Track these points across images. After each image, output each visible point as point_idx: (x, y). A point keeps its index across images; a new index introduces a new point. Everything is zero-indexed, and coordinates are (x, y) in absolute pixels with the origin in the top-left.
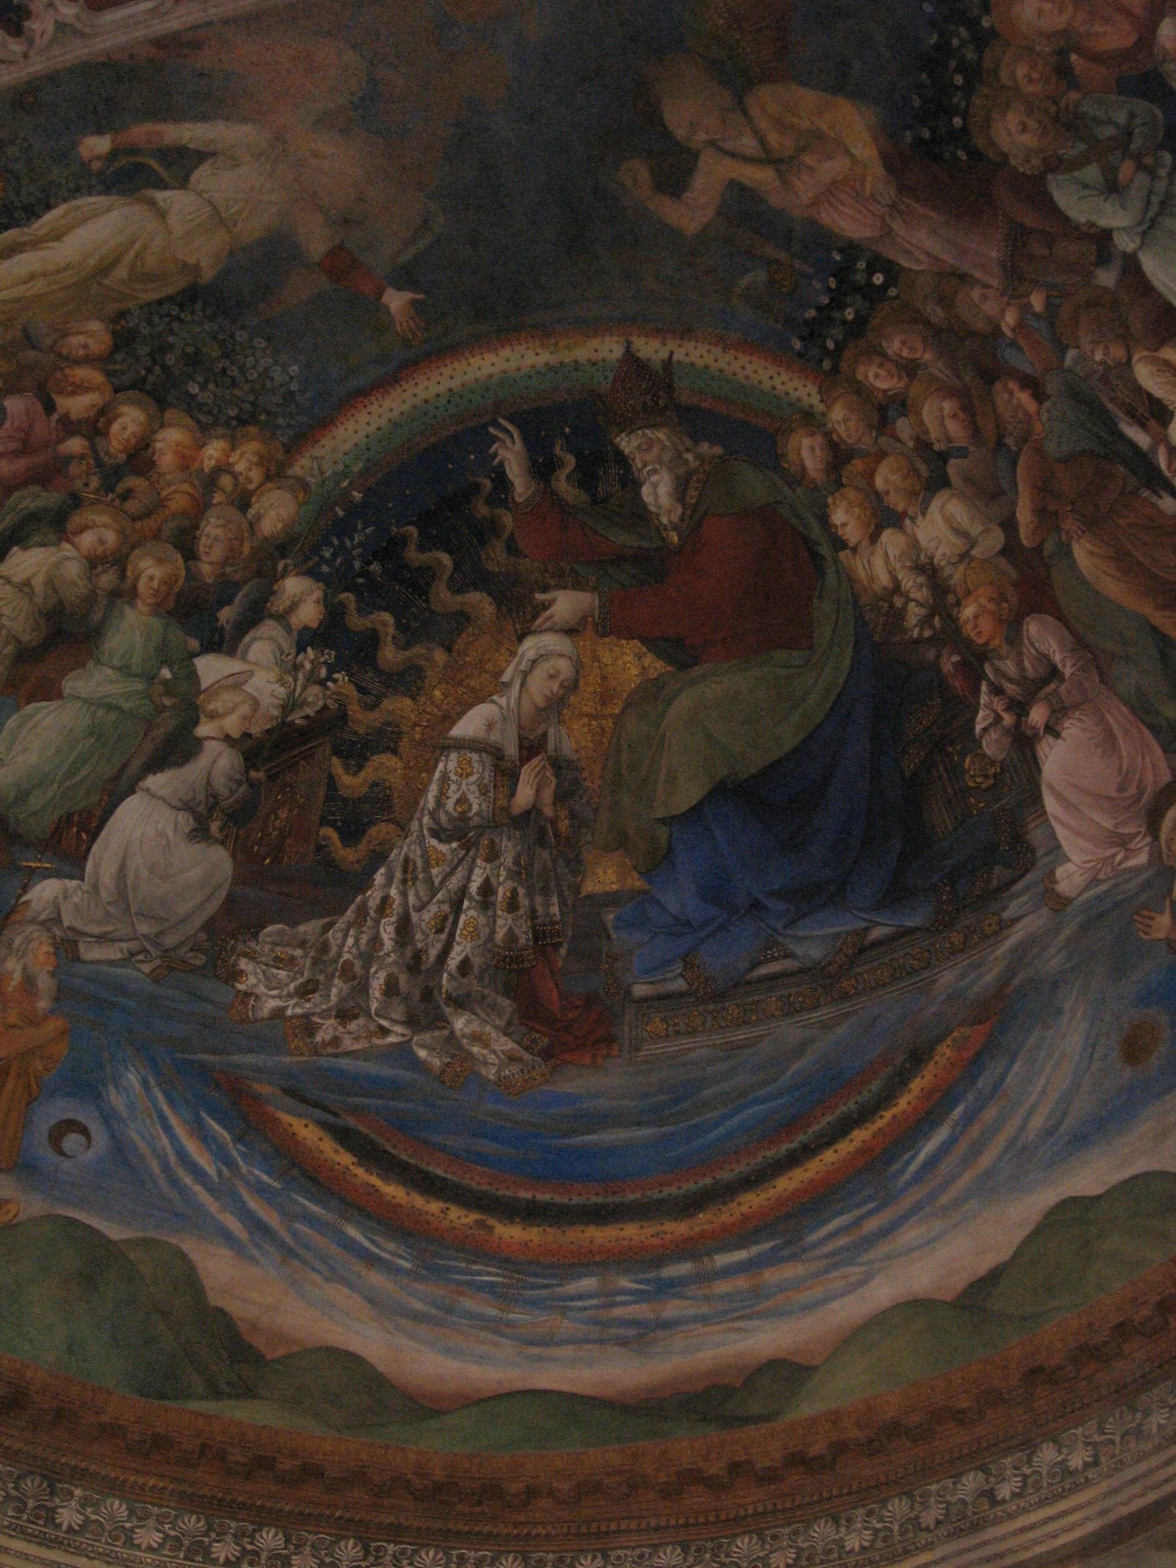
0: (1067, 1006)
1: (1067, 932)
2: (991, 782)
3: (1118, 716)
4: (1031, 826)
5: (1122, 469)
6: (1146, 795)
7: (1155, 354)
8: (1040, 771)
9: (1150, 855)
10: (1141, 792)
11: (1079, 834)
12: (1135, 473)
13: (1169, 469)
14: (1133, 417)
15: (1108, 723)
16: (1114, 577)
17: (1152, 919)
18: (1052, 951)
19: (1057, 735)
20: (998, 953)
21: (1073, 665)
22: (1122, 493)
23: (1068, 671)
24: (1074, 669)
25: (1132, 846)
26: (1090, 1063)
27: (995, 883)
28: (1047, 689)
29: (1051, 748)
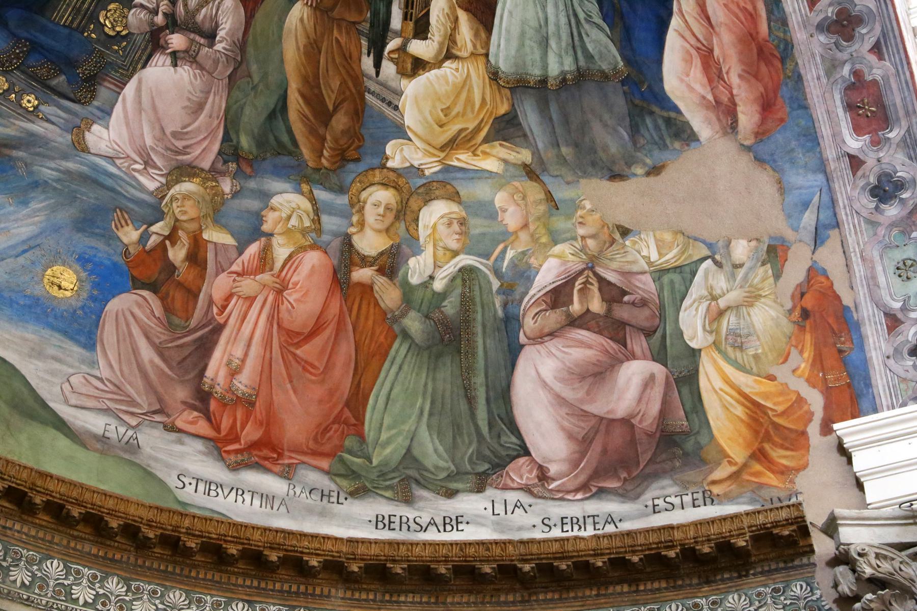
0: (34, 205)
1: (71, 165)
2: (112, 33)
3: (217, 102)
4: (106, 84)
5: (369, 15)
6: (185, 157)
7: (456, 6)
8: (144, 67)
9: (158, 189)
10: (184, 151)
11: (127, 124)
12: (372, 26)
13: (390, 53)
14: (407, 6)
15: (207, 98)
16: (298, 49)
17: (127, 225)
18: (53, 165)
19: (175, 65)
20: (17, 122)
21: (224, 48)
22: (354, 23)
23: (219, 47)
24: (223, 51)
25: (151, 171)
26: (17, 257)
27: (54, 83)
28: (198, 38)
29: (163, 65)
